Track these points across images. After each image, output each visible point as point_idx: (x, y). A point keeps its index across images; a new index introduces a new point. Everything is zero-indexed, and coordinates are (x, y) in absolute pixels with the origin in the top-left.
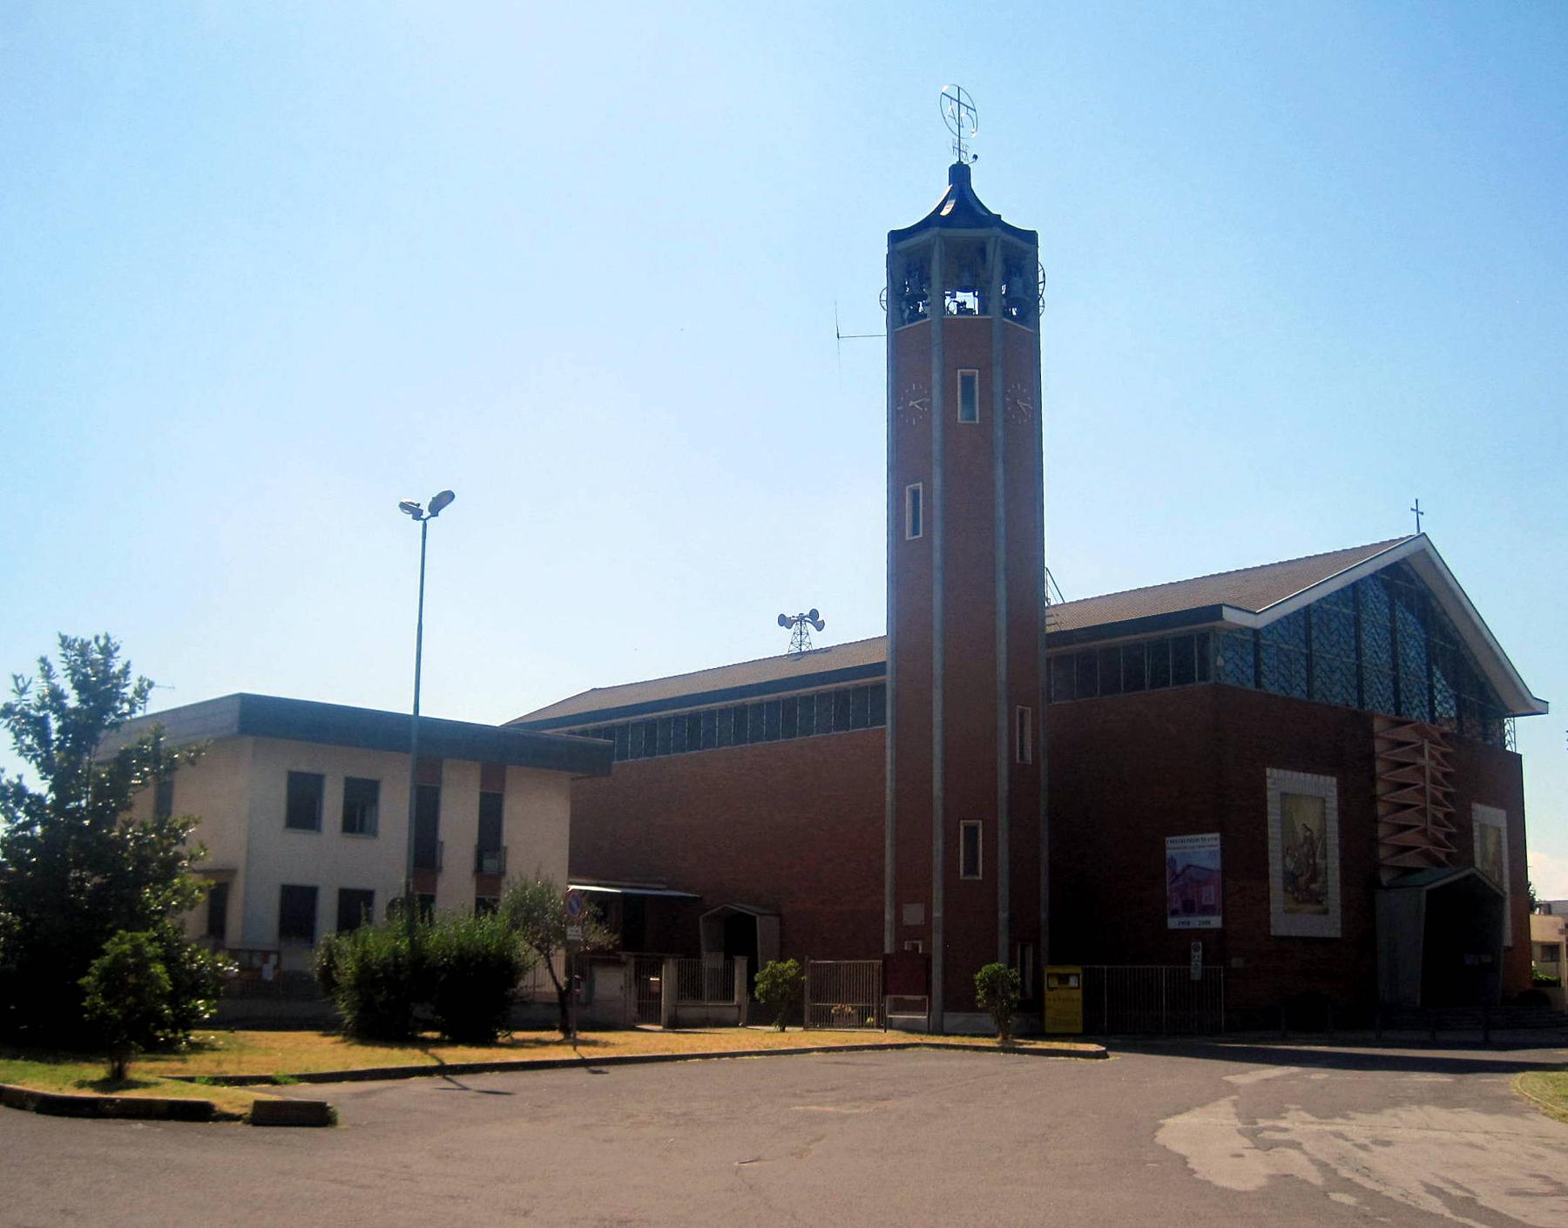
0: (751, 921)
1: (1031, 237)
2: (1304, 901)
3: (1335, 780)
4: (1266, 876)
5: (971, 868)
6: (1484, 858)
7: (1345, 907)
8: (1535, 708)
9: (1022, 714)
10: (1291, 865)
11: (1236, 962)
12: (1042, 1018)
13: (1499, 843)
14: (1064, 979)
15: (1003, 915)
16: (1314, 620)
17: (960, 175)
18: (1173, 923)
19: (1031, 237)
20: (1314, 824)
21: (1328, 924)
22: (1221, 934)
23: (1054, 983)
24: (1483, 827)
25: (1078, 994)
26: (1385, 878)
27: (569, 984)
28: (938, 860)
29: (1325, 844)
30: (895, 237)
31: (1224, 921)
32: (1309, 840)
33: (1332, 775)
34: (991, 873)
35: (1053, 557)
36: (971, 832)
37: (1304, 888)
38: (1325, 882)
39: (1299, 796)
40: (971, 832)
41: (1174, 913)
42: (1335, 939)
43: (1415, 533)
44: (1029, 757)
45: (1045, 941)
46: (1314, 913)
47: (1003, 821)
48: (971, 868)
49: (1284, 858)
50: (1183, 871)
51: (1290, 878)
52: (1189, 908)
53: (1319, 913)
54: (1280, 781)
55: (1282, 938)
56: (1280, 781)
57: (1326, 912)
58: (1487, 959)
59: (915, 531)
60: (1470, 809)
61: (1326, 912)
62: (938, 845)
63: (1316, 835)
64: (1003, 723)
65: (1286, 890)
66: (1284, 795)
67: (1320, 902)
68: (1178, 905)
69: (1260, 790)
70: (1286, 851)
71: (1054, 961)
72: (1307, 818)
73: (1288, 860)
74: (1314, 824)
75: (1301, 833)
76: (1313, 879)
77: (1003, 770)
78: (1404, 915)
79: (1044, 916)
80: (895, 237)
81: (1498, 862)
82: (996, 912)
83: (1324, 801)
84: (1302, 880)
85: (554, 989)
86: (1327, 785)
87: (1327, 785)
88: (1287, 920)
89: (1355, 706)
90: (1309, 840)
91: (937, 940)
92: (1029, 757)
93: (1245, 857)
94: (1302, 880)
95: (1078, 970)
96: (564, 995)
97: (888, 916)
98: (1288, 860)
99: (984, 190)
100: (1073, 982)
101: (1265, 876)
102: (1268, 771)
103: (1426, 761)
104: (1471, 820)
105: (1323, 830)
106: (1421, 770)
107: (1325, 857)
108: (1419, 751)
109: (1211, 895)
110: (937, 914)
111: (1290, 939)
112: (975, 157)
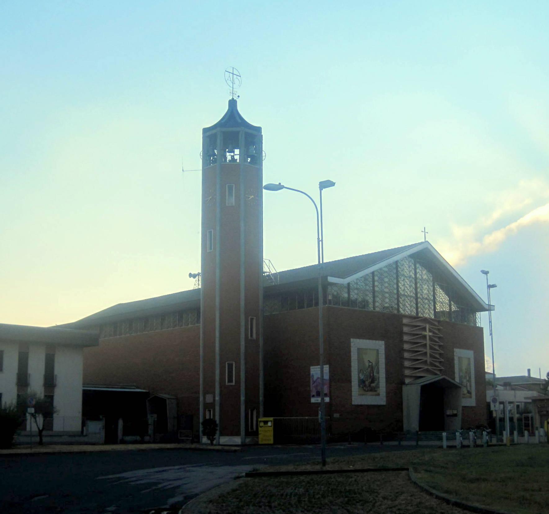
0: (166, 400)
1: (259, 129)
2: (367, 391)
3: (383, 342)
5: (230, 380)
6: (460, 370)
7: (388, 393)
8: (489, 308)
9: (252, 319)
10: (362, 377)
11: (336, 415)
12: (258, 438)
13: (469, 364)
14: (266, 422)
15: (243, 398)
16: (376, 278)
17: (233, 104)
18: (313, 400)
19: (259, 129)
21: (379, 399)
22: (330, 404)
23: (262, 424)
24: (460, 358)
25: (272, 429)
26: (407, 381)
27: (43, 429)
28: (217, 378)
29: (378, 368)
30: (205, 130)
31: (331, 399)
32: (371, 367)
33: (382, 340)
34: (238, 381)
35: (266, 255)
36: (230, 366)
37: (369, 384)
38: (379, 382)
39: (366, 349)
40: (230, 366)
41: (313, 396)
42: (383, 406)
43: (423, 241)
44: (254, 336)
45: (261, 409)
47: (243, 362)
48: (230, 380)
49: (359, 375)
50: (316, 380)
51: (362, 382)
52: (318, 394)
53: (376, 395)
54: (356, 344)
56: (356, 344)
57: (379, 395)
58: (455, 412)
59: (211, 249)
60: (453, 352)
61: (379, 395)
62: (217, 372)
63: (374, 363)
64: (243, 323)
65: (359, 386)
66: (358, 349)
67: (375, 391)
68: (314, 393)
69: (349, 347)
70: (360, 371)
71: (265, 416)
72: (370, 358)
73: (360, 375)
75: (367, 364)
76: (373, 382)
77: (243, 343)
78: (412, 396)
79: (261, 398)
80: (205, 130)
81: (468, 372)
82: (240, 397)
83: (378, 350)
85: (37, 430)
86: (380, 345)
87: (380, 345)
88: (358, 398)
89: (396, 312)
90: (371, 367)
91: (217, 408)
92: (254, 336)
93: (340, 376)
94: (367, 383)
95: (272, 419)
96: (40, 432)
97: (201, 399)
98: (360, 375)
99: (241, 109)
100: (269, 424)
101: (350, 381)
102: (352, 340)
103: (428, 333)
104: (453, 355)
105: (377, 363)
106: (425, 337)
107: (378, 373)
108: (424, 329)
109: (326, 390)
110: (217, 398)
111: (361, 405)
112: (239, 96)
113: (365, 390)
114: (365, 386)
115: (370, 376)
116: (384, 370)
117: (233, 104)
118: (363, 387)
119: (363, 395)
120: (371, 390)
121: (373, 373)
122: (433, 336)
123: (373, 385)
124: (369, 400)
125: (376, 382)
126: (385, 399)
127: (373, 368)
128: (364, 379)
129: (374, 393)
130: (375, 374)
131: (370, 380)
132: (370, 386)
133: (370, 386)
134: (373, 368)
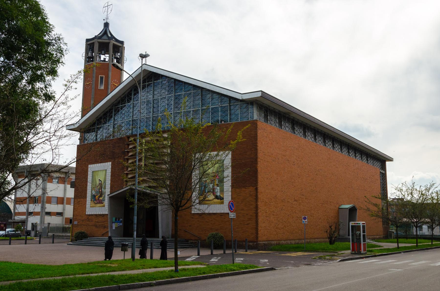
4: (86, 198)
20: (102, 180)
29: (105, 185)
46: (100, 207)
49: (92, 191)
51: (93, 197)
55: (90, 215)
57: (104, 206)
61: (104, 206)
65: (91, 200)
66: (93, 172)
67: (102, 203)
72: (100, 177)
74: (102, 180)
75: (98, 182)
76: (101, 196)
84: (97, 197)
94: (97, 197)
101: (85, 197)
107: (105, 188)
115: (100, 192)
116: (110, 186)
118: (94, 201)
119: (93, 207)
120: (99, 203)
121: (102, 189)
123: (101, 198)
127: (101, 186)
129: (102, 205)
132: (98, 199)
133: (98, 199)
134: (101, 186)
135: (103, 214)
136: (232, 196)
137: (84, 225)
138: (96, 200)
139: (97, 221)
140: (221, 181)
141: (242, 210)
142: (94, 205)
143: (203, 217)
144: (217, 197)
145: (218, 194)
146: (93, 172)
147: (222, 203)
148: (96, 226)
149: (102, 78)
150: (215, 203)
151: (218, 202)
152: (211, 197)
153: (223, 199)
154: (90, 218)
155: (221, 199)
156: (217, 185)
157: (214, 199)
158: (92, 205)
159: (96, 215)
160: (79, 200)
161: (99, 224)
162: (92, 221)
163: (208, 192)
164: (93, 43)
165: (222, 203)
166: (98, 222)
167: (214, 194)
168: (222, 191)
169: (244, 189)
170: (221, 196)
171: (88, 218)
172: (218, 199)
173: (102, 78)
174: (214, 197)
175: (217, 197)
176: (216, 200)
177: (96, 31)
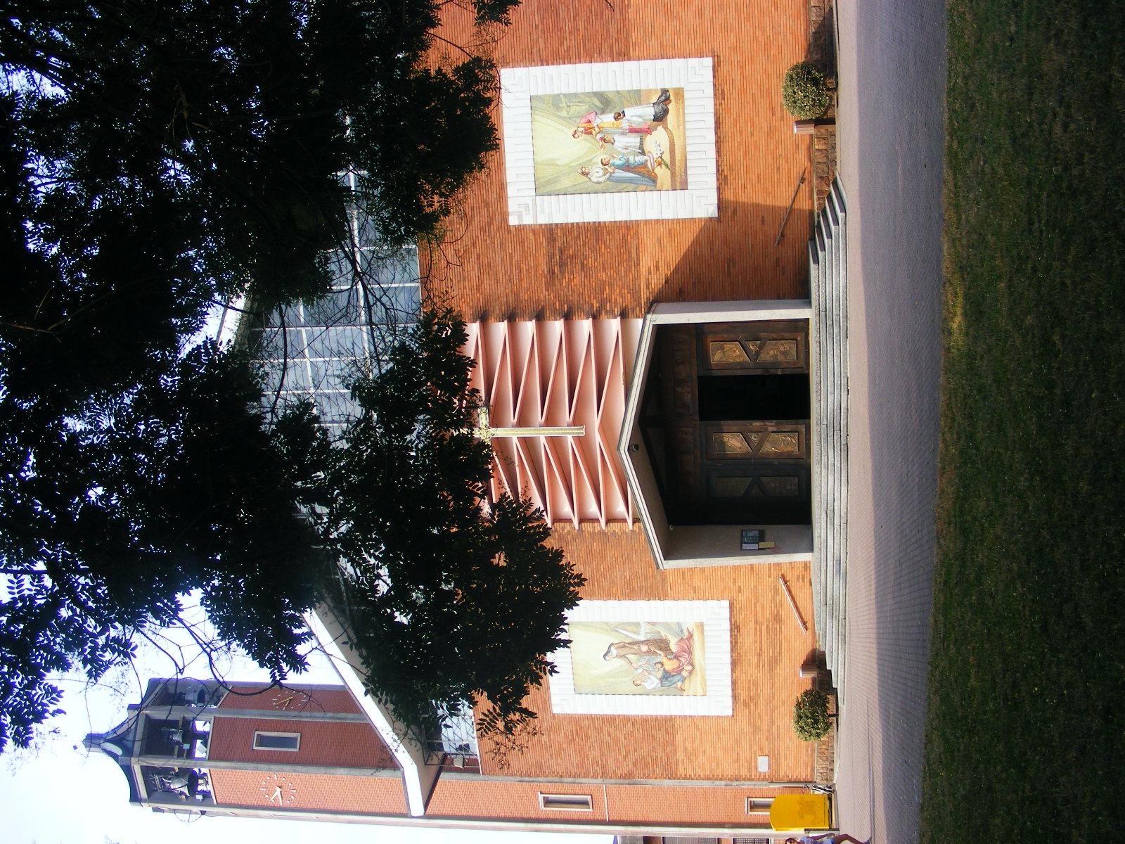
2: (692, 664)
10: (653, 682)
17: (93, 740)
20: (604, 641)
38: (666, 625)
46: (703, 648)
53: (702, 632)
55: (735, 697)
61: (701, 626)
66: (577, 691)
67: (691, 636)
75: (615, 663)
76: (663, 645)
84: (670, 665)
94: (670, 665)
101: (666, 724)
112: (75, 748)
113: (691, 672)
114: (679, 670)
115: (649, 652)
117: (93, 740)
118: (684, 679)
119: (704, 679)
120: (689, 651)
122: (487, 404)
124: (714, 656)
125: (664, 634)
126: (712, 604)
128: (660, 674)
130: (642, 638)
131: (661, 657)
132: (677, 657)
135: (731, 630)
136: (655, 58)
137: (772, 722)
138: (679, 670)
139: (754, 660)
140: (604, 102)
141: (700, 13)
142: (697, 678)
143: (731, 169)
144: (660, 118)
145: (649, 112)
146: (577, 691)
147: (680, 93)
148: (774, 662)
149: (263, 741)
150: (682, 122)
151: (678, 110)
152: (657, 142)
153: (665, 91)
154: (743, 695)
155: (668, 99)
156: (619, 116)
157: (666, 128)
158: (700, 692)
159: (734, 664)
160: (680, 755)
161: (765, 647)
162: (756, 684)
163: (643, 153)
164: (147, 771)
165: (680, 93)
166: (760, 655)
167: (648, 131)
168: (637, 97)
169: (631, 13)
170: (655, 99)
171: (746, 705)
172: (666, 111)
173: (263, 741)
174: (660, 128)
175: (660, 118)
176: (671, 118)
177: (107, 773)
